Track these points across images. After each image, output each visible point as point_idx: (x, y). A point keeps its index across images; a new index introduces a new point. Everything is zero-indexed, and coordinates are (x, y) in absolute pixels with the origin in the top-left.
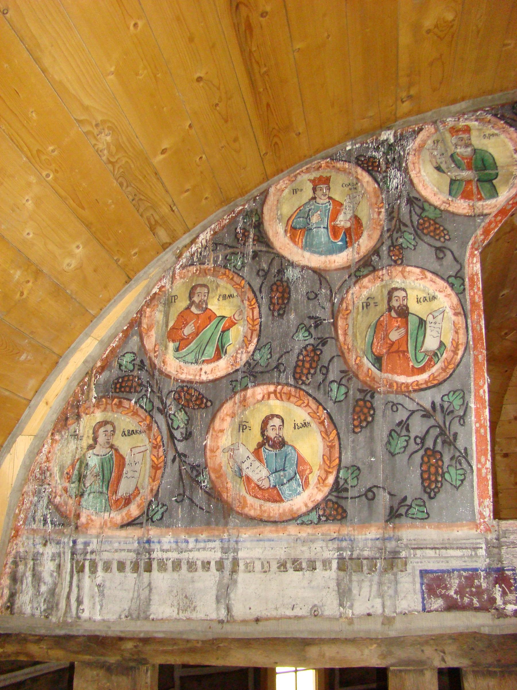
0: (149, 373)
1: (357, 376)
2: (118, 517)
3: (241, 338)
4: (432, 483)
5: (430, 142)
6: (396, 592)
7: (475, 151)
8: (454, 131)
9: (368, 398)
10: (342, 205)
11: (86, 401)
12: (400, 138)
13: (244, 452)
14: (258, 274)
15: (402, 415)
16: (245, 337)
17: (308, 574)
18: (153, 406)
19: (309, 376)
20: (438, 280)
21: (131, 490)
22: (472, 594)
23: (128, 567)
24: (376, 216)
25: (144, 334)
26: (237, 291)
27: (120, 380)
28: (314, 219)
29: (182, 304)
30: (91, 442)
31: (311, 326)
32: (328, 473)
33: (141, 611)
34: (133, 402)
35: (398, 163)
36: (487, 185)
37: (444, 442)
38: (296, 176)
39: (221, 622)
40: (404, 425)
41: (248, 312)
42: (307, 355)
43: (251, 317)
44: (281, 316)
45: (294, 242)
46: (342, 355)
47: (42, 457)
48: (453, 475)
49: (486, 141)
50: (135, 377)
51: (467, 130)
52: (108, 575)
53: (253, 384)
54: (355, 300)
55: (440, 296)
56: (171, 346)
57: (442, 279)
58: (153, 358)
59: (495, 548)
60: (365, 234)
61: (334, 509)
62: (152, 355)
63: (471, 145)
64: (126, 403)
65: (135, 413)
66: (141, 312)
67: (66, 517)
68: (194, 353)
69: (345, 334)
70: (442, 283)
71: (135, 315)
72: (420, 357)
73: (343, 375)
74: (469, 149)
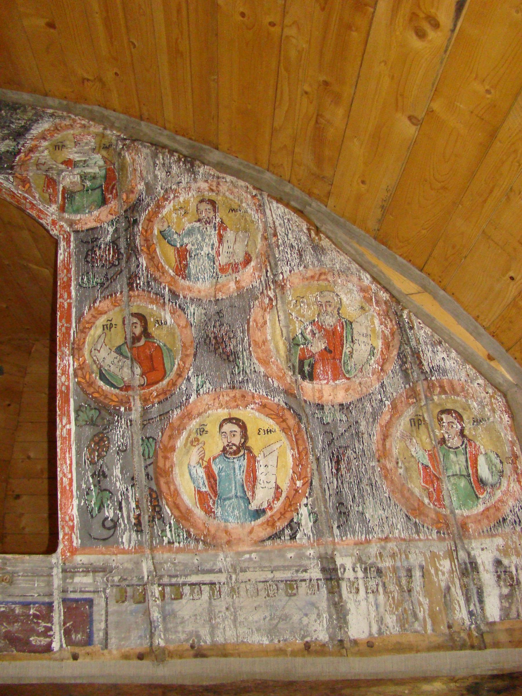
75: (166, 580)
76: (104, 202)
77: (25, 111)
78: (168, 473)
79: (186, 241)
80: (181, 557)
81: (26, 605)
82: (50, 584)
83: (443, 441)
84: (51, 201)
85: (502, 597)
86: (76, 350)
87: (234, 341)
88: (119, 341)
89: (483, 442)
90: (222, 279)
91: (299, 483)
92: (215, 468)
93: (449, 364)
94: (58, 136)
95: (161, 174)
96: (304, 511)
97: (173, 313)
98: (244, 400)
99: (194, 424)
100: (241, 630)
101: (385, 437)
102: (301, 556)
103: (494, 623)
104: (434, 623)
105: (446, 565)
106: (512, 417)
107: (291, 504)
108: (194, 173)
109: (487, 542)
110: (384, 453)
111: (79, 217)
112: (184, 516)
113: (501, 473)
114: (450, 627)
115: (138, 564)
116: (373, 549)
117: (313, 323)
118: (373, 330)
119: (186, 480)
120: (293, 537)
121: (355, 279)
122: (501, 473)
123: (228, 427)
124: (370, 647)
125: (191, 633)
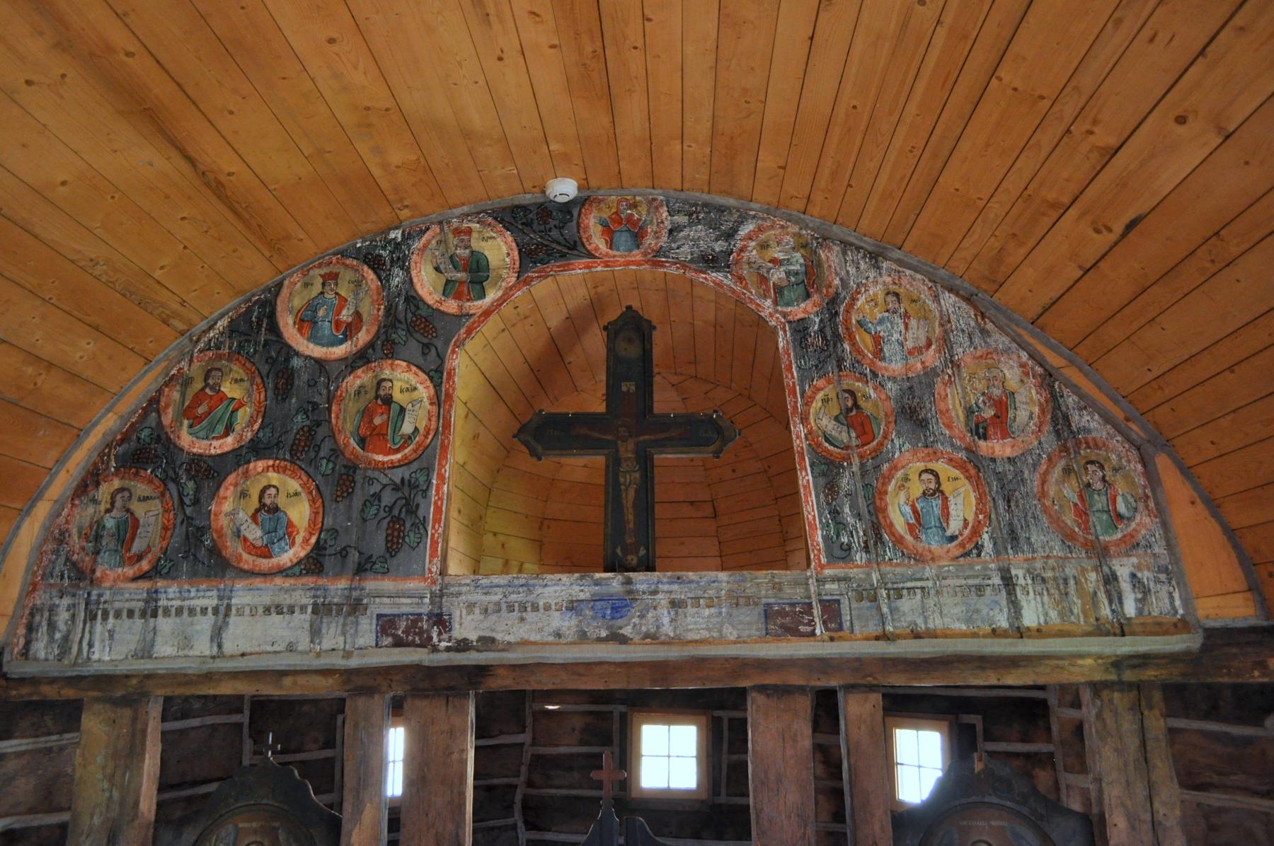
2: (130, 571)
3: (247, 418)
4: (394, 545)
5: (434, 242)
6: (356, 631)
7: (472, 252)
8: (457, 232)
12: (407, 237)
13: (242, 516)
15: (376, 488)
17: (287, 617)
20: (420, 373)
21: (144, 547)
22: (415, 634)
23: (137, 614)
28: (321, 313)
29: (198, 385)
30: (108, 506)
32: (311, 534)
33: (146, 651)
35: (402, 262)
36: (478, 287)
37: (407, 512)
39: (213, 657)
40: (377, 496)
41: (255, 395)
44: (284, 400)
45: (302, 334)
46: (333, 436)
47: (62, 519)
48: (412, 538)
49: (483, 244)
51: (469, 231)
52: (119, 621)
55: (420, 387)
56: (186, 422)
59: (438, 597)
60: (364, 328)
61: (314, 564)
62: (168, 430)
63: (470, 247)
64: (142, 473)
65: (150, 482)
66: (160, 391)
67: (83, 572)
69: (337, 417)
75: (890, 585)
76: (808, 296)
77: (731, 213)
78: (884, 510)
79: (879, 328)
80: (898, 570)
81: (793, 605)
82: (808, 590)
83: (1089, 485)
84: (765, 297)
85: (1137, 600)
86: (804, 419)
87: (924, 411)
88: (836, 412)
89: (1121, 487)
90: (911, 361)
91: (981, 517)
92: (918, 506)
93: (1093, 425)
94: (762, 237)
95: (852, 270)
96: (986, 536)
97: (875, 389)
98: (936, 456)
99: (900, 474)
100: (946, 620)
101: (1044, 482)
102: (986, 568)
103: (1130, 619)
104: (1085, 616)
105: (1093, 576)
106: (1144, 465)
107: (976, 532)
108: (879, 268)
109: (1125, 560)
110: (1043, 494)
111: (789, 309)
112: (899, 541)
113: (1136, 509)
114: (1097, 620)
115: (869, 575)
116: (1038, 564)
117: (983, 394)
118: (1031, 399)
119: (898, 515)
120: (979, 555)
121: (1015, 357)
122: (1136, 509)
123: (925, 476)
124: (1039, 633)
125: (910, 623)
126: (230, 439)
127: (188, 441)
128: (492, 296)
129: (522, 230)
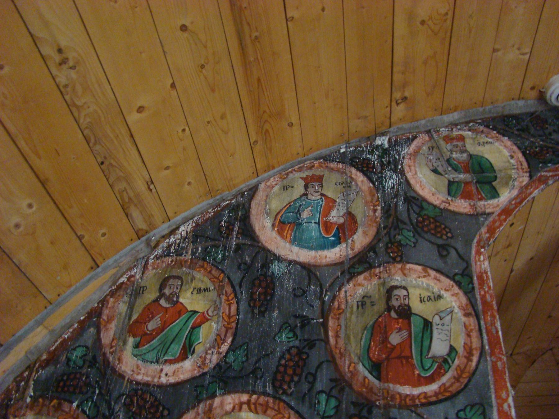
0: (100, 371)
1: (350, 387)
3: (212, 337)
7: (471, 156)
8: (448, 139)
9: (365, 413)
10: (335, 201)
11: (18, 401)
12: (395, 144)
14: (239, 267)
16: (218, 335)
18: (98, 411)
19: (292, 385)
20: (443, 278)
24: (371, 213)
25: (102, 327)
26: (214, 285)
27: (65, 378)
28: (305, 215)
29: (150, 296)
31: (296, 326)
34: (75, 404)
35: (395, 165)
36: (487, 187)
38: (287, 174)
42: (291, 360)
43: (227, 313)
44: (262, 313)
45: (282, 237)
46: (332, 361)
49: (481, 148)
50: (83, 375)
51: (462, 138)
53: (223, 391)
54: (349, 298)
56: (131, 341)
57: (448, 277)
58: (108, 354)
60: (360, 231)
62: (107, 350)
63: (466, 151)
64: (66, 406)
66: (103, 302)
68: (155, 351)
69: (337, 336)
70: (447, 282)
71: (96, 305)
72: (427, 364)
73: (334, 384)
74: (465, 155)
126: (188, 364)
127: (131, 365)
128: (506, 196)
129: (519, 135)
